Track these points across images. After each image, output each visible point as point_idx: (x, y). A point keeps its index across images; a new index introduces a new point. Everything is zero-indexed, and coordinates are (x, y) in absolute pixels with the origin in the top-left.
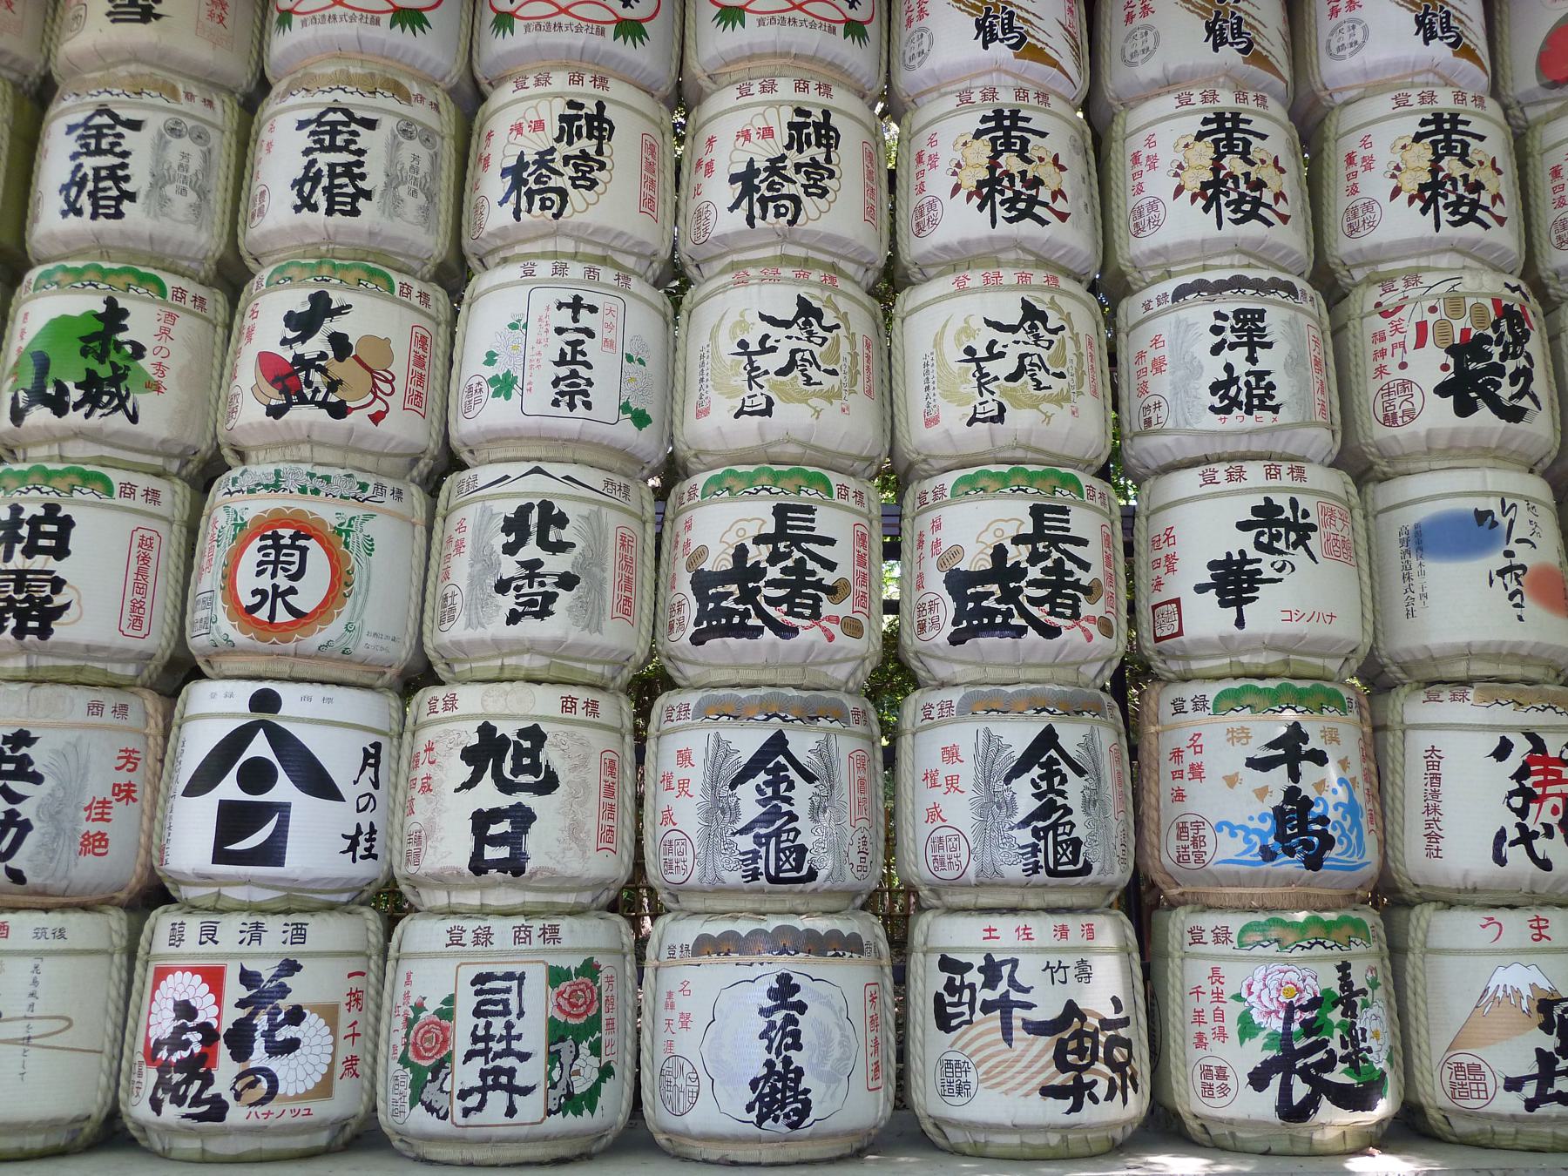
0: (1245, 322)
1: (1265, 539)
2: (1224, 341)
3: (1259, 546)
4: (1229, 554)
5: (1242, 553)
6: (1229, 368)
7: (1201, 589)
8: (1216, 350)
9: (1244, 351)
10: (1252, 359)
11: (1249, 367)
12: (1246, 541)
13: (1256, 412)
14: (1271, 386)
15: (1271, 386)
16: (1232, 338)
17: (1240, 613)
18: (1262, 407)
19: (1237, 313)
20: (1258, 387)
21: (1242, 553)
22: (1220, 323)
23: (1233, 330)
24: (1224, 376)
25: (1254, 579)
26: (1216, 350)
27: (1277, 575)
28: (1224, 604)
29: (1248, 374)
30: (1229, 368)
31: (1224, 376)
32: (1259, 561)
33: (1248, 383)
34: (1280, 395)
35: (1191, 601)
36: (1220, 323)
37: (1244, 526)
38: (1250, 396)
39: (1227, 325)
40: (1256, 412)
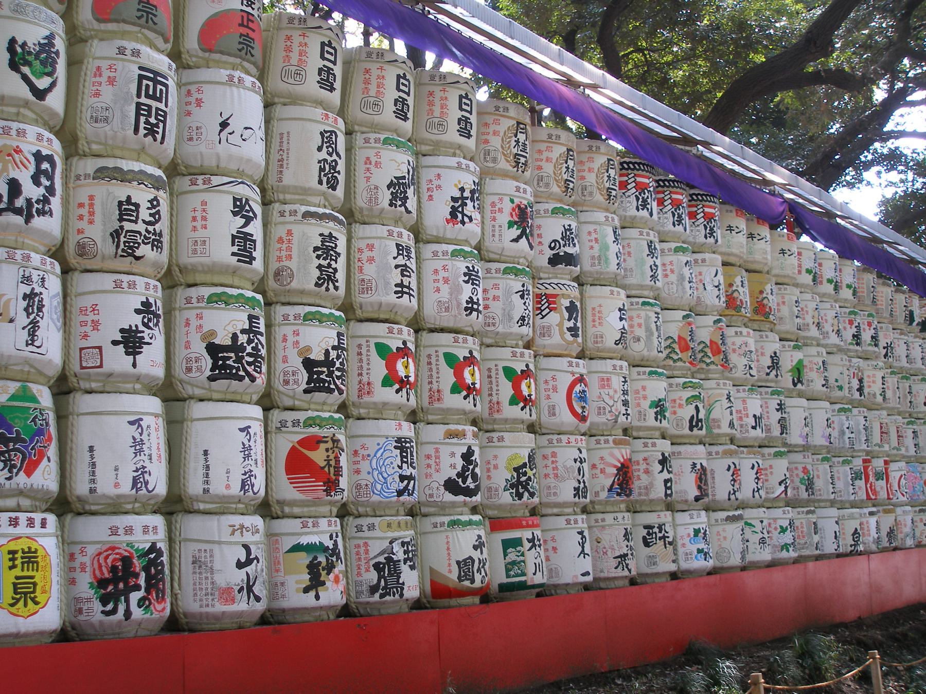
1: (146, 320)
3: (144, 324)
4: (130, 326)
5: (136, 326)
7: (115, 343)
12: (137, 320)
17: (135, 358)
21: (136, 326)
25: (141, 343)
27: (150, 341)
28: (127, 353)
32: (143, 332)
35: (108, 349)
37: (138, 311)
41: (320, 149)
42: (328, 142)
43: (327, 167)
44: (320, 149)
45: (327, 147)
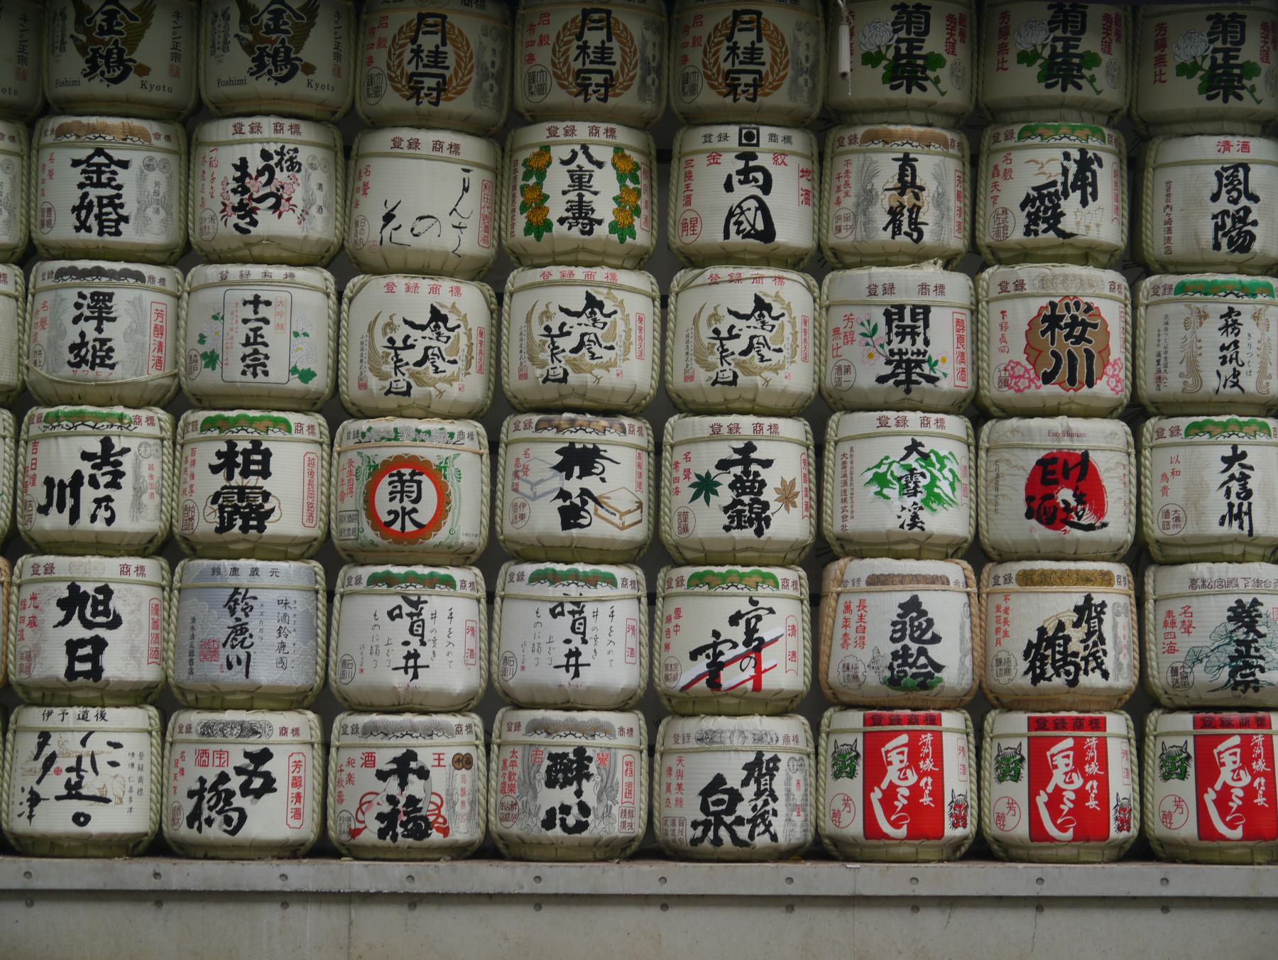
0: (98, 301)
2: (81, 315)
6: (82, 335)
8: (76, 320)
9: (94, 323)
10: (99, 330)
11: (96, 335)
13: (97, 369)
14: (111, 350)
15: (111, 350)
16: (87, 313)
18: (102, 365)
19: (93, 295)
20: (101, 350)
22: (81, 301)
23: (89, 307)
24: (78, 340)
26: (76, 320)
29: (95, 340)
30: (82, 335)
31: (78, 340)
33: (94, 347)
34: (116, 356)
36: (81, 301)
38: (94, 356)
39: (86, 303)
40: (97, 369)
41: (1215, 197)
42: (1231, 183)
43: (1229, 222)
44: (1215, 197)
45: (1228, 192)
